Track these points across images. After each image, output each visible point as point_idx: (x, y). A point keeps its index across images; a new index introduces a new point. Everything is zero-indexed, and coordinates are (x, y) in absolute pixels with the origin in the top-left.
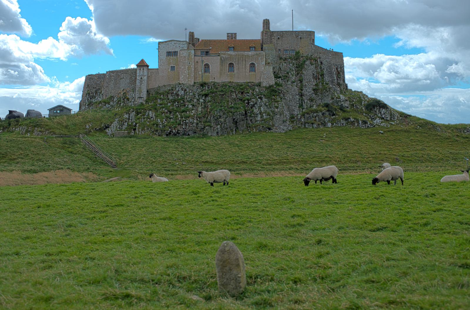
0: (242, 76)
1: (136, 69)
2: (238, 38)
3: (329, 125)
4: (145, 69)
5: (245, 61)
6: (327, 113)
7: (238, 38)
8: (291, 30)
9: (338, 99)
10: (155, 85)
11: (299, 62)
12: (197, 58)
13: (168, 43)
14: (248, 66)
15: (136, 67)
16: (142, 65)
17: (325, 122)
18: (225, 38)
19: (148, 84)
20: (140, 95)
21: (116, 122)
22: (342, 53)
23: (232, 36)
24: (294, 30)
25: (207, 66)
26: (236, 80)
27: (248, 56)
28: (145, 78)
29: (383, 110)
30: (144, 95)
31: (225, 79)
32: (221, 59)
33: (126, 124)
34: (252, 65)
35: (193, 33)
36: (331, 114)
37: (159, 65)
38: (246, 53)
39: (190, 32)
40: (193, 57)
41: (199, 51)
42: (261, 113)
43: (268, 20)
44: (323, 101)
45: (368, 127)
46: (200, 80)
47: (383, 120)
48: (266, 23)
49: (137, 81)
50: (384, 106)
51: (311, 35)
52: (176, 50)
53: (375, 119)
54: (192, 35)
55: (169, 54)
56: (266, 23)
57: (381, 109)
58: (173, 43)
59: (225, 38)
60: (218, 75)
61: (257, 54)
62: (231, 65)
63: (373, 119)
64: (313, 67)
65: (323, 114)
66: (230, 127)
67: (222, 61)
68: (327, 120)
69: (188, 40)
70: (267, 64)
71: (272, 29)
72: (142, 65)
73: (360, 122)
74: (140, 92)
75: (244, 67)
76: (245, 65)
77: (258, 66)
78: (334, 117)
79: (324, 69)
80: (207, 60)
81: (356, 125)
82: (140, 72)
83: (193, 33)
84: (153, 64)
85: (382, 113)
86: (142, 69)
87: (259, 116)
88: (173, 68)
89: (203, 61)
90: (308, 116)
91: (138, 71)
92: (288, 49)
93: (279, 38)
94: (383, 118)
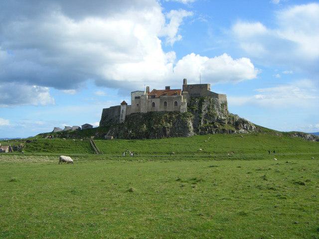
2: (171, 88)
7: (171, 88)
10: (128, 114)
16: (124, 103)
20: (123, 118)
25: (154, 104)
27: (173, 98)
28: (125, 110)
30: (124, 118)
31: (162, 109)
48: (185, 81)
50: (246, 122)
55: (136, 98)
56: (185, 81)
60: (159, 107)
62: (165, 103)
71: (188, 83)
72: (124, 103)
74: (122, 117)
80: (154, 100)
84: (129, 103)
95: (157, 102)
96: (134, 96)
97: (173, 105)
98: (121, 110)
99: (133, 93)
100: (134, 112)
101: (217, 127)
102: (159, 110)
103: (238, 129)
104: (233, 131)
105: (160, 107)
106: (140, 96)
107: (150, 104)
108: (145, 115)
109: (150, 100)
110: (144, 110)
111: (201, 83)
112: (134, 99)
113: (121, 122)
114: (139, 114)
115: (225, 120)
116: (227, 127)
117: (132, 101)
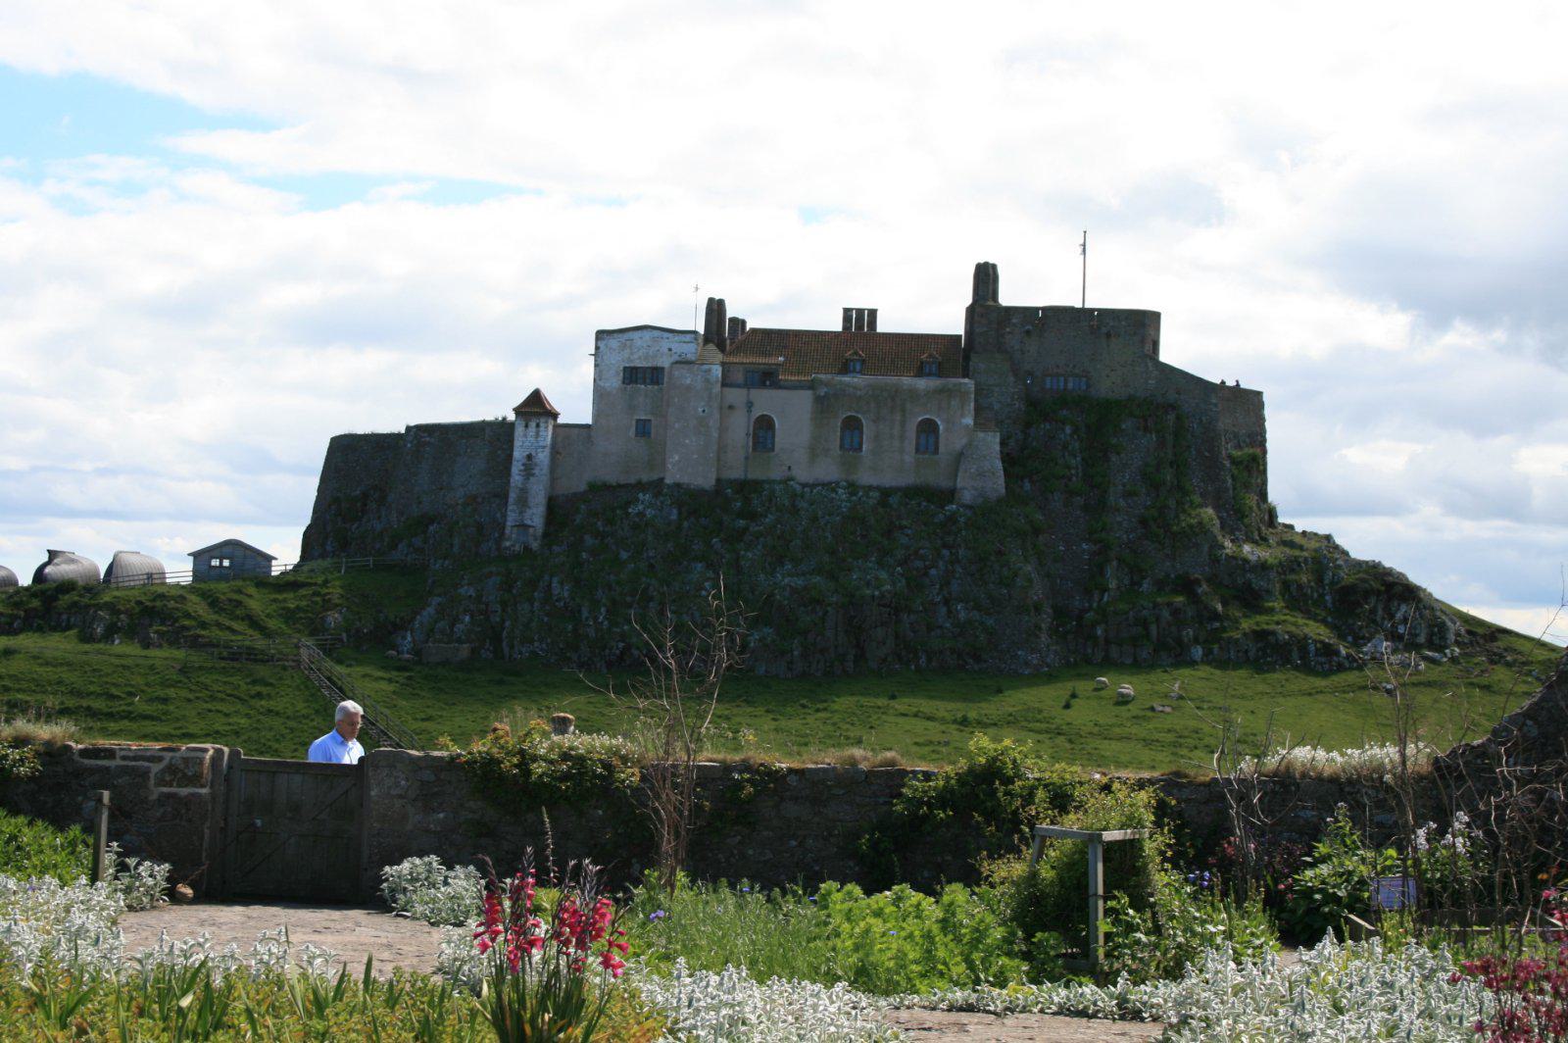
0: (889, 462)
1: (512, 425)
2: (883, 326)
5: (903, 411)
7: (883, 326)
8: (1079, 305)
10: (575, 483)
11: (1101, 419)
13: (630, 335)
15: (511, 417)
16: (535, 407)
17: (1179, 642)
18: (837, 325)
19: (553, 479)
21: (431, 610)
22: (1259, 394)
23: (860, 321)
24: (1088, 305)
25: (765, 425)
26: (865, 477)
27: (913, 395)
28: (543, 457)
29: (1404, 608)
30: (536, 516)
31: (827, 470)
34: (928, 428)
35: (721, 303)
37: (597, 414)
38: (907, 381)
39: (711, 301)
40: (717, 388)
41: (741, 368)
42: (946, 602)
43: (994, 267)
46: (736, 473)
48: (986, 277)
49: (516, 469)
51: (1142, 326)
52: (659, 365)
54: (715, 308)
55: (632, 375)
56: (986, 277)
58: (647, 335)
59: (837, 325)
62: (852, 425)
63: (1363, 638)
66: (836, 647)
67: (824, 405)
69: (701, 330)
70: (981, 423)
71: (1009, 295)
72: (535, 407)
74: (523, 502)
76: (903, 423)
80: (766, 401)
82: (525, 436)
83: (721, 303)
84: (575, 406)
85: (1399, 615)
87: (944, 610)
88: (643, 429)
89: (750, 405)
91: (519, 431)
93: (1028, 332)
95: (792, 413)
96: (617, 360)
97: (910, 445)
98: (518, 454)
99: (614, 343)
100: (611, 476)
101: (1216, 616)
102: (802, 474)
103: (1358, 641)
104: (1328, 651)
105: (814, 452)
106: (665, 362)
107: (740, 429)
108: (690, 500)
109: (736, 396)
110: (688, 463)
111: (1095, 302)
112: (614, 382)
113: (512, 541)
114: (657, 486)
115: (1263, 567)
116: (1285, 622)
117: (600, 395)
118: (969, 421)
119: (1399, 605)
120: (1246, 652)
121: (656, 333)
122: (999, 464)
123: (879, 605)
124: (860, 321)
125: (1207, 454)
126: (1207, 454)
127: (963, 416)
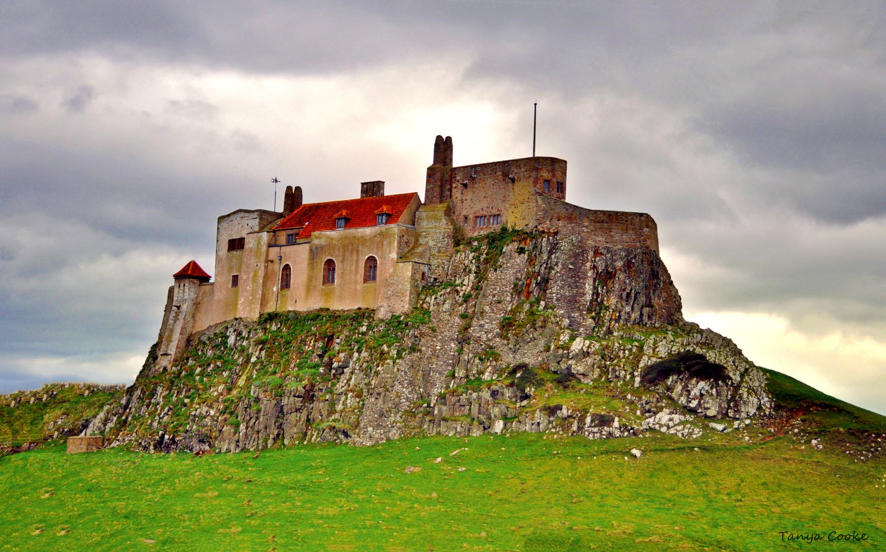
3: (499, 426)
4: (187, 285)
6: (508, 393)
7: (388, 191)
9: (560, 351)
12: (274, 251)
14: (362, 264)
18: (356, 194)
27: (363, 240)
29: (702, 384)
32: (311, 250)
33: (115, 418)
34: (372, 263)
36: (519, 394)
39: (289, 188)
40: (264, 248)
44: (518, 357)
45: (610, 434)
47: (690, 418)
48: (443, 147)
53: (655, 413)
56: (443, 147)
57: (694, 381)
59: (356, 194)
61: (381, 234)
62: (330, 264)
63: (649, 411)
64: (521, 260)
65: (494, 394)
67: (314, 254)
68: (495, 411)
69: (280, 209)
73: (588, 420)
75: (353, 268)
76: (357, 262)
77: (381, 263)
78: (525, 403)
79: (557, 264)
81: (575, 428)
85: (695, 392)
86: (182, 285)
90: (454, 399)
92: (485, 213)
94: (693, 411)
118: (394, 255)
119: (698, 382)
120: (539, 424)
121: (243, 214)
122: (408, 286)
123: (294, 396)
124: (372, 189)
125: (571, 267)
126: (571, 267)
127: (390, 252)
